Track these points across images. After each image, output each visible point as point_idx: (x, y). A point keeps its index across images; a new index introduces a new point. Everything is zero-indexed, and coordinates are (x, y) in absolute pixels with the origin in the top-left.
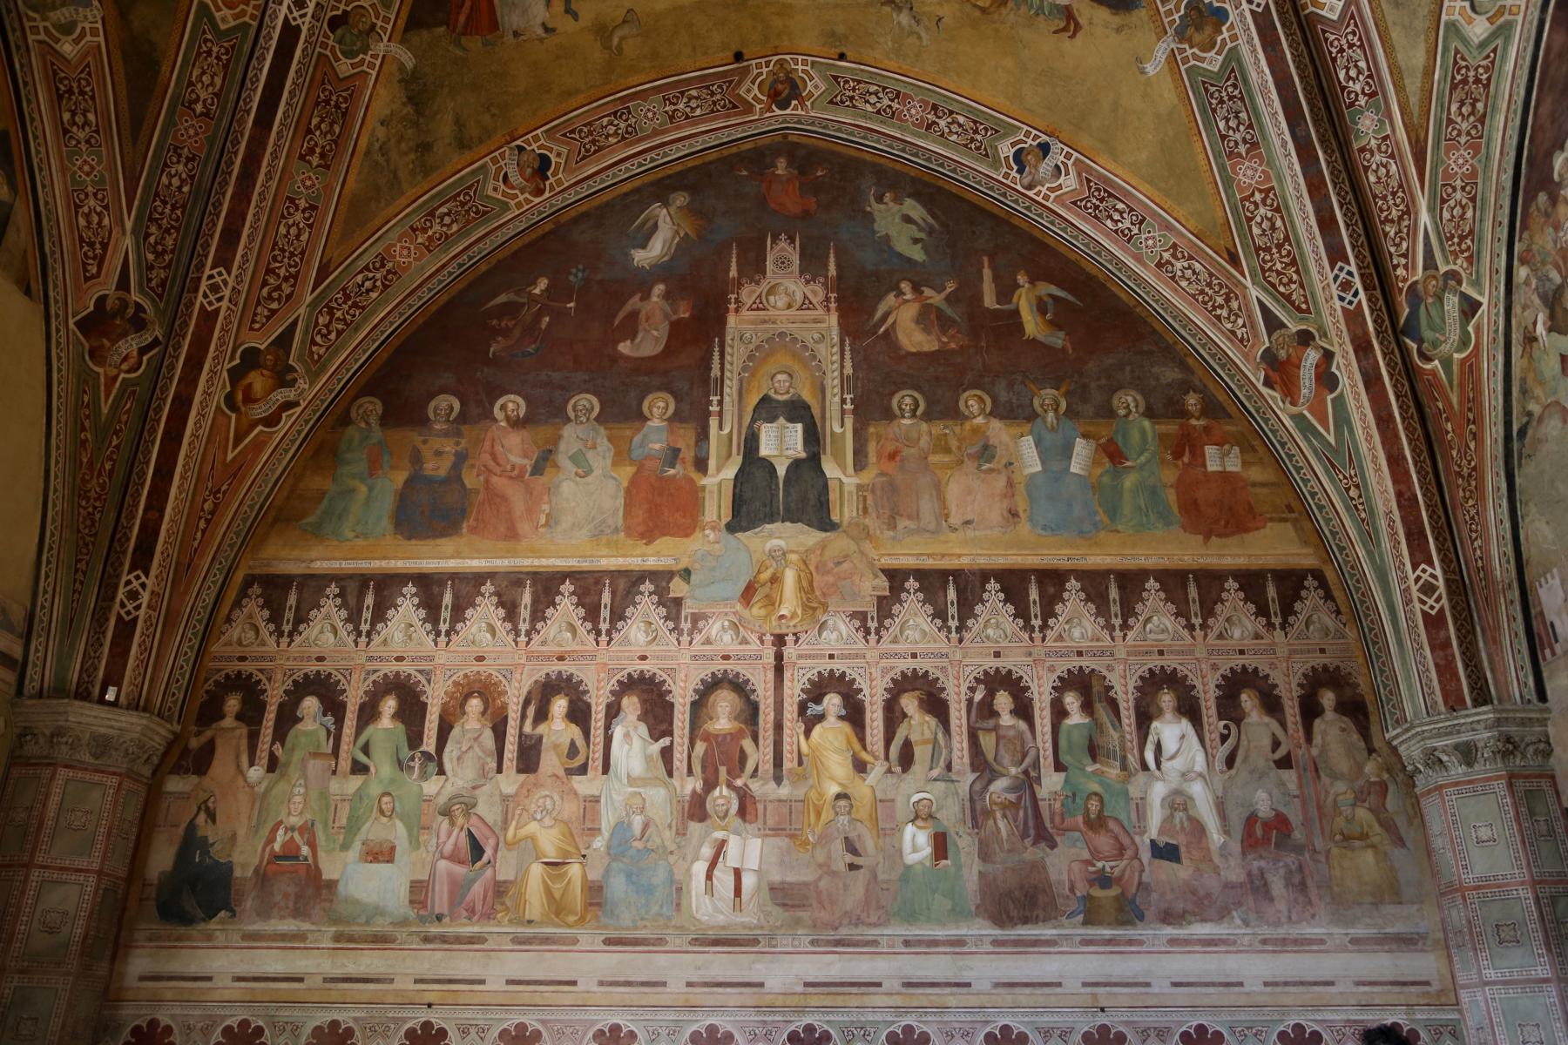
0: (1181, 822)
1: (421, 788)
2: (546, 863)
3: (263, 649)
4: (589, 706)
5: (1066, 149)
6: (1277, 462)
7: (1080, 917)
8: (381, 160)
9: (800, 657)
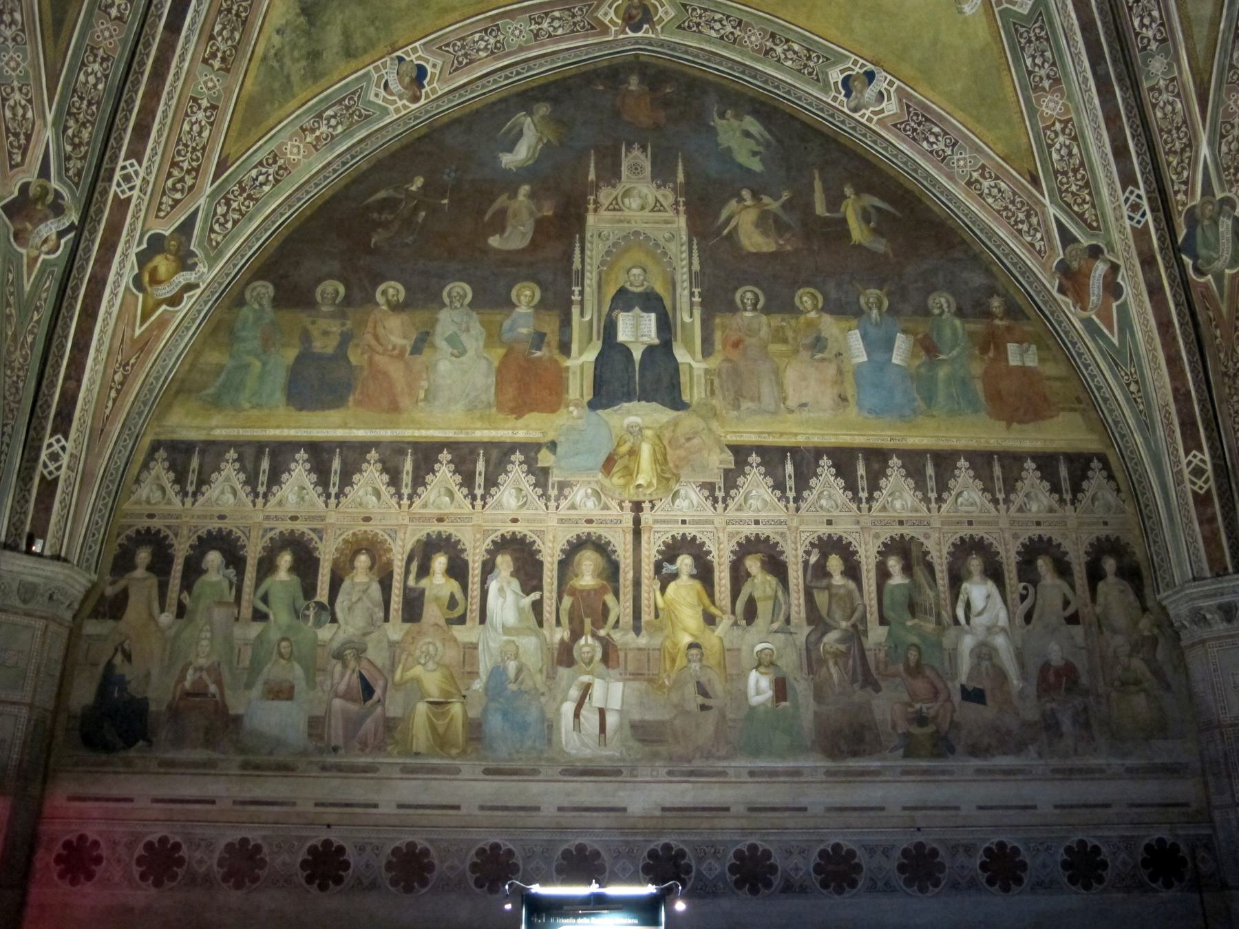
1: (316, 636)
2: (431, 703)
3: (168, 507)
4: (466, 563)
5: (889, 77)
6: (1069, 360)
7: (901, 751)
8: (276, 65)
9: (656, 522)
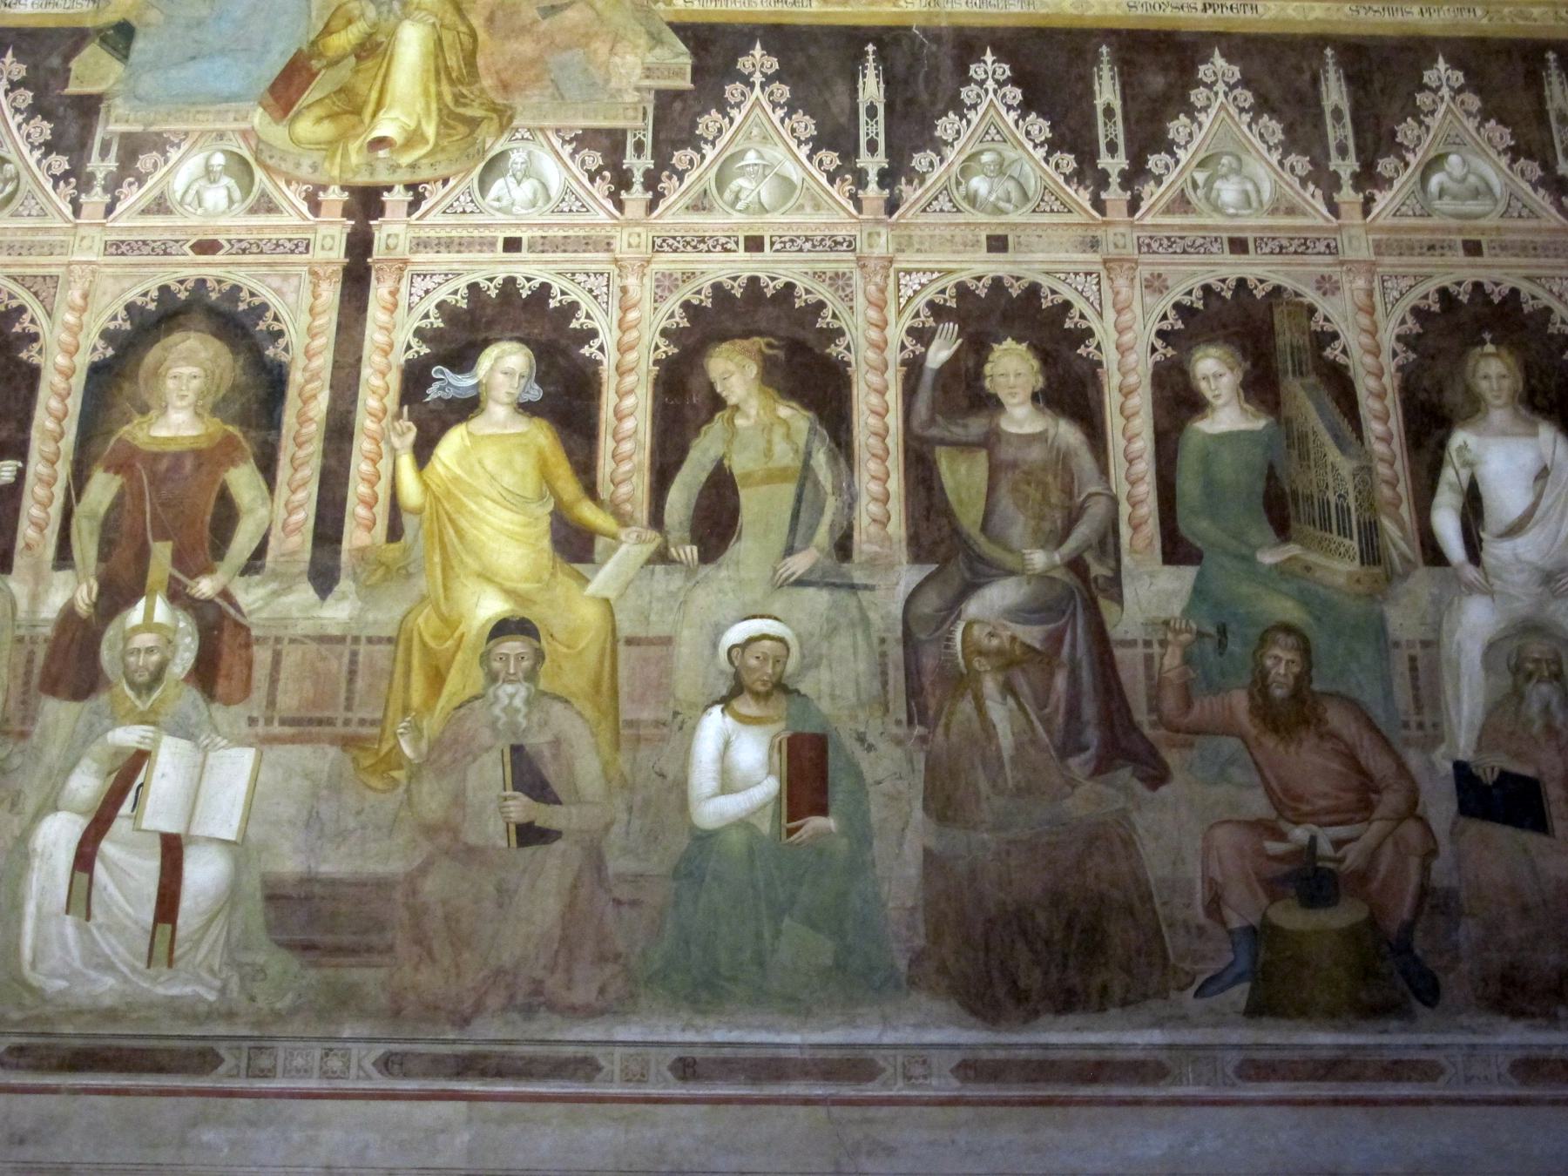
0: (1546, 709)
7: (1239, 994)
9: (421, 244)
